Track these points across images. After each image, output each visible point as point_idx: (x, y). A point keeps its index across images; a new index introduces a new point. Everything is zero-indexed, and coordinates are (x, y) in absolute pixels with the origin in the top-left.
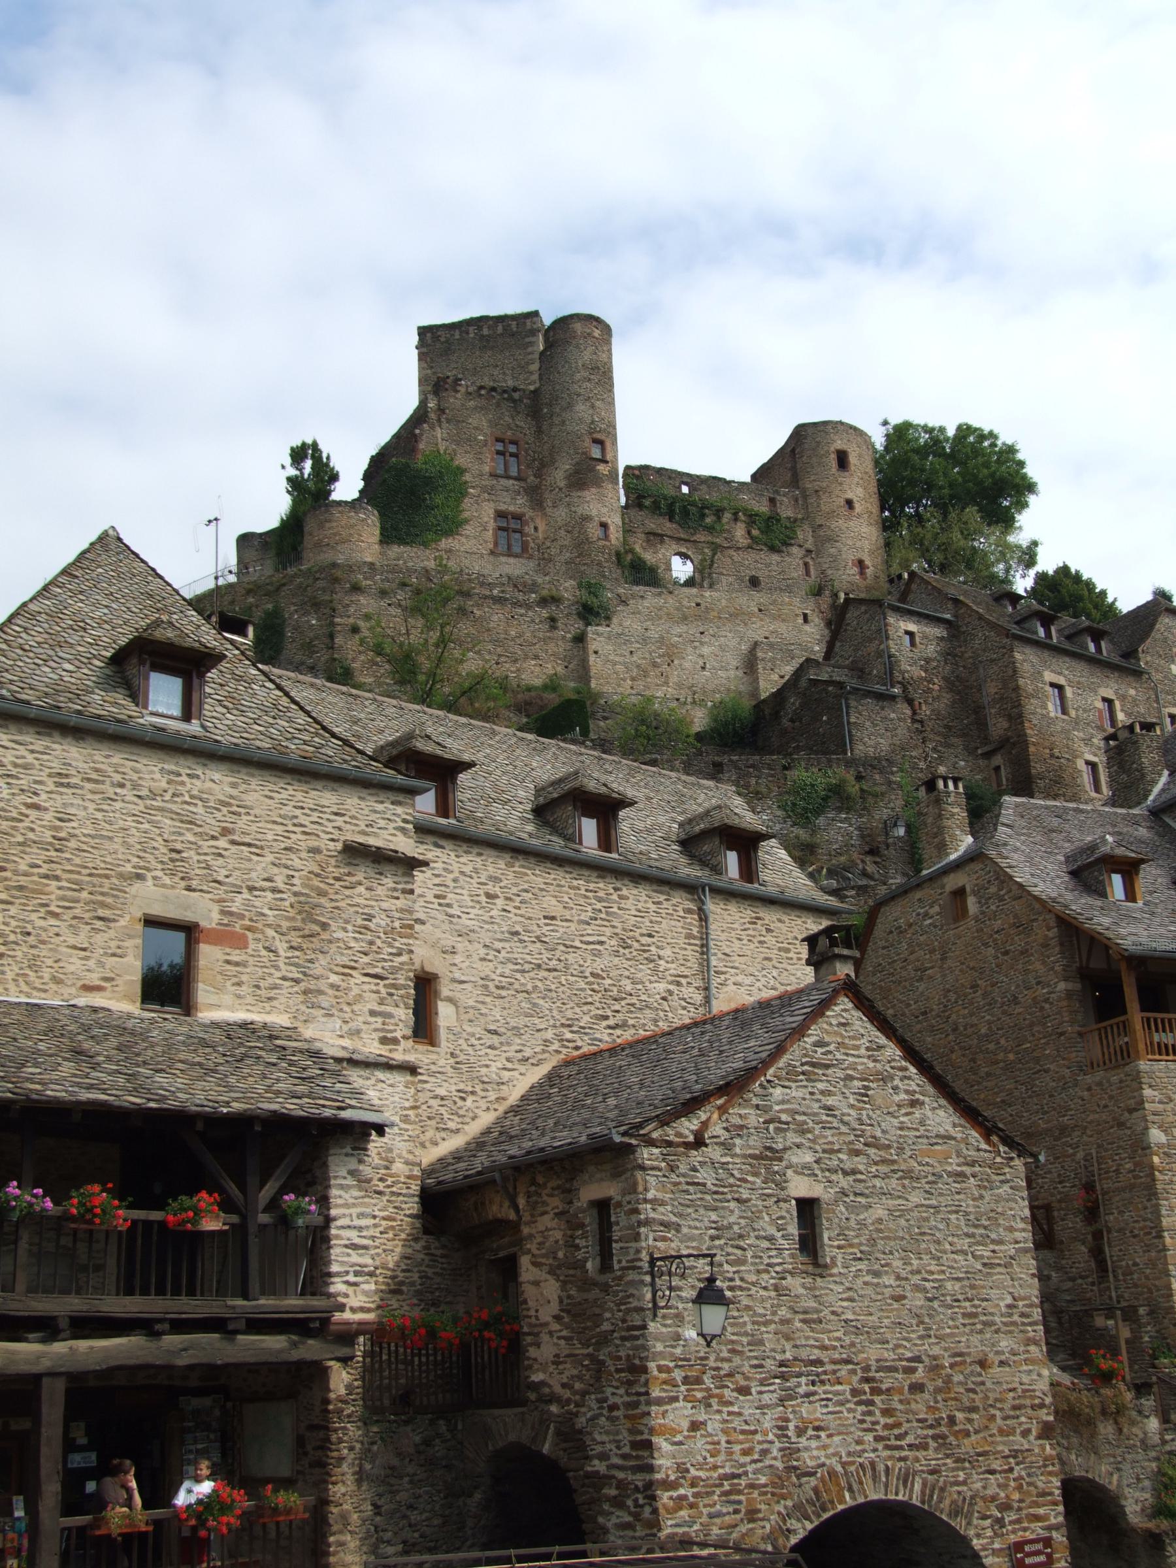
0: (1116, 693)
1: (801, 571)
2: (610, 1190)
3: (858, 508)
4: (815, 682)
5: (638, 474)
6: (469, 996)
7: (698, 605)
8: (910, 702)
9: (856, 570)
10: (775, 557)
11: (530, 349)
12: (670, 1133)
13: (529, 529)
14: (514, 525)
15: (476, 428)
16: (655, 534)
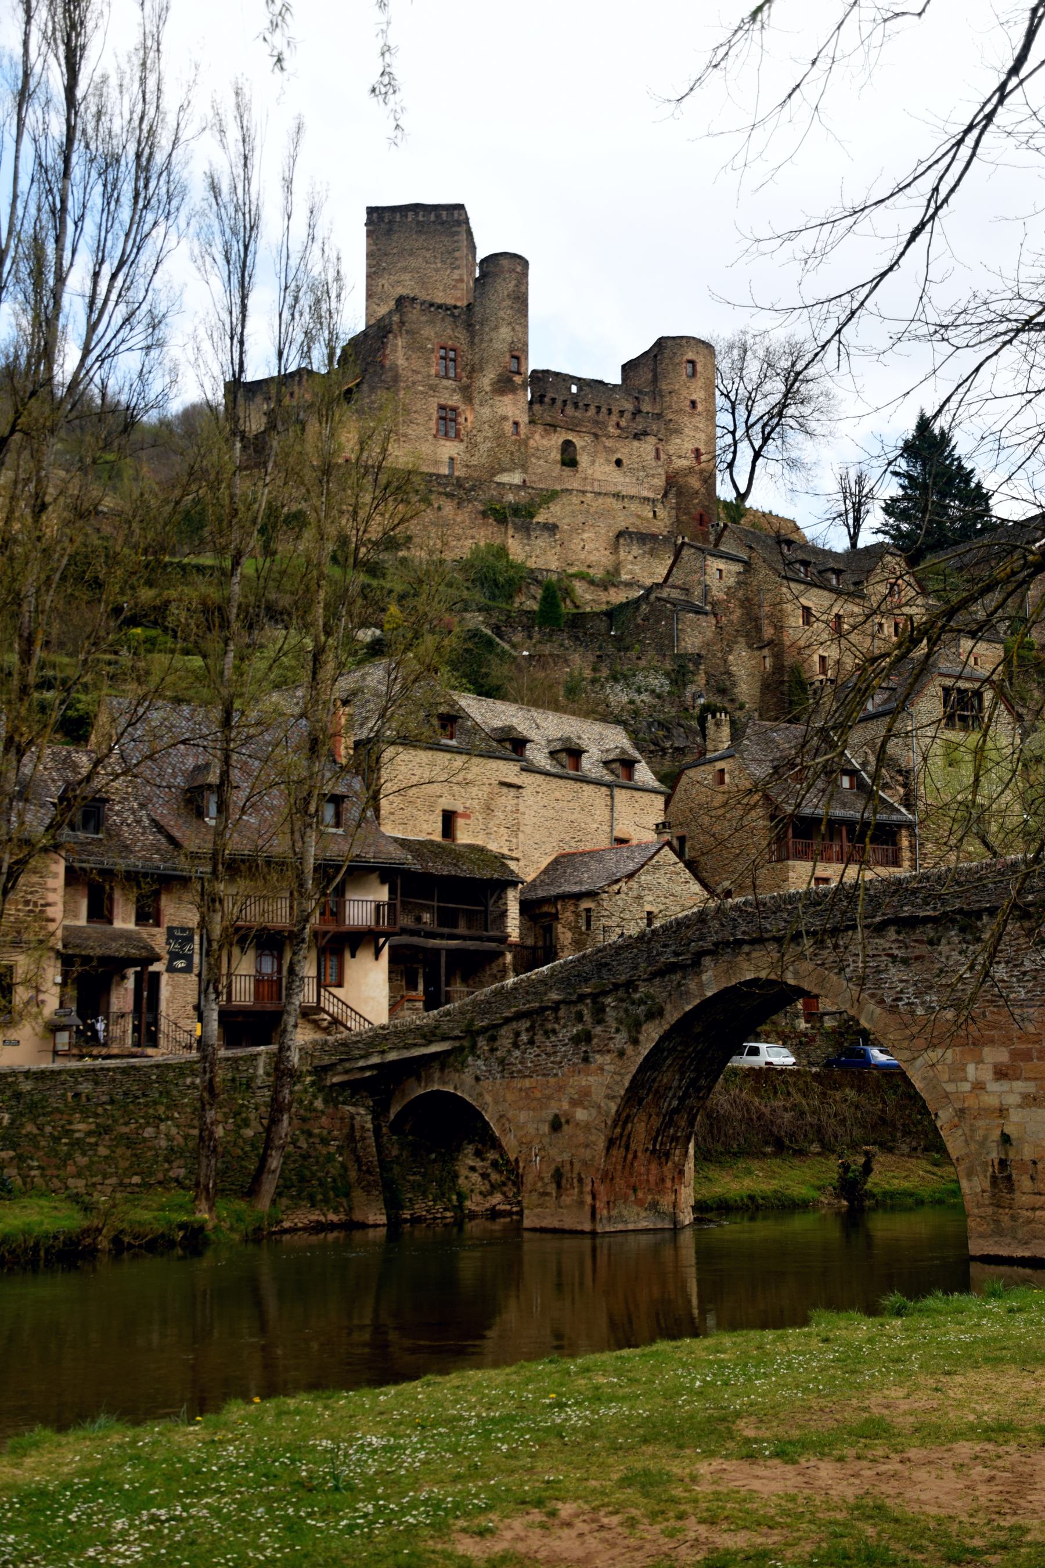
1: (653, 454)
2: (591, 905)
3: (700, 408)
4: (658, 599)
5: (541, 377)
6: (528, 830)
8: (715, 615)
12: (610, 889)
13: (461, 420)
14: (451, 415)
15: (427, 339)
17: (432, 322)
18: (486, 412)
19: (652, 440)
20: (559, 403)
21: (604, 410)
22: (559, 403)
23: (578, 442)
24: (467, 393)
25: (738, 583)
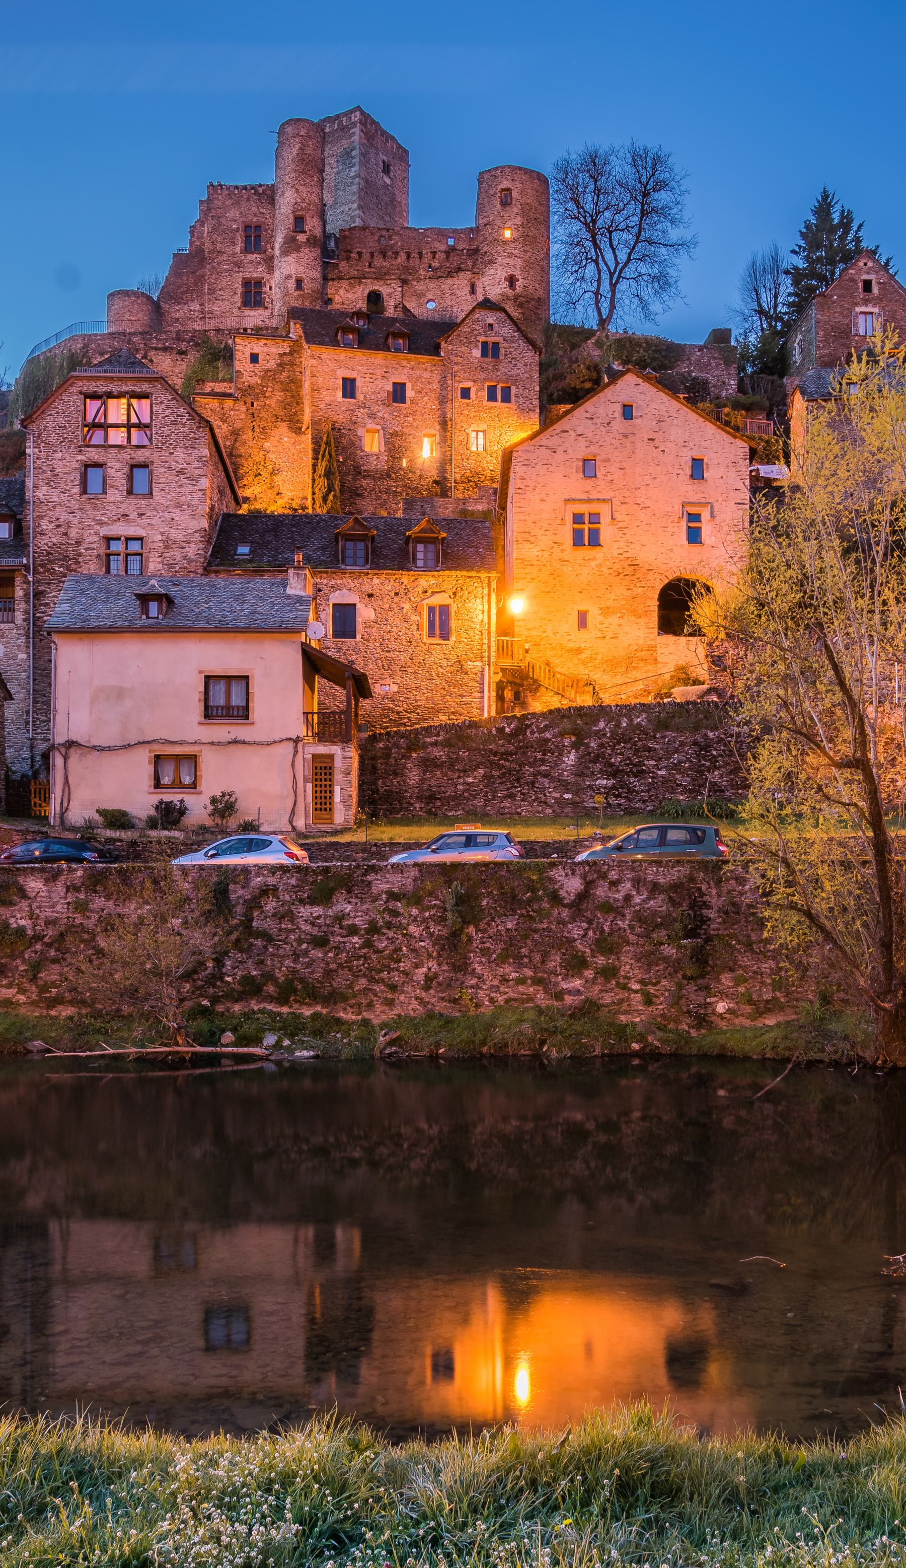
0: (410, 378)
13: (266, 289)
17: (237, 203)
20: (366, 256)
21: (415, 255)
22: (366, 256)
23: (384, 290)
25: (280, 365)
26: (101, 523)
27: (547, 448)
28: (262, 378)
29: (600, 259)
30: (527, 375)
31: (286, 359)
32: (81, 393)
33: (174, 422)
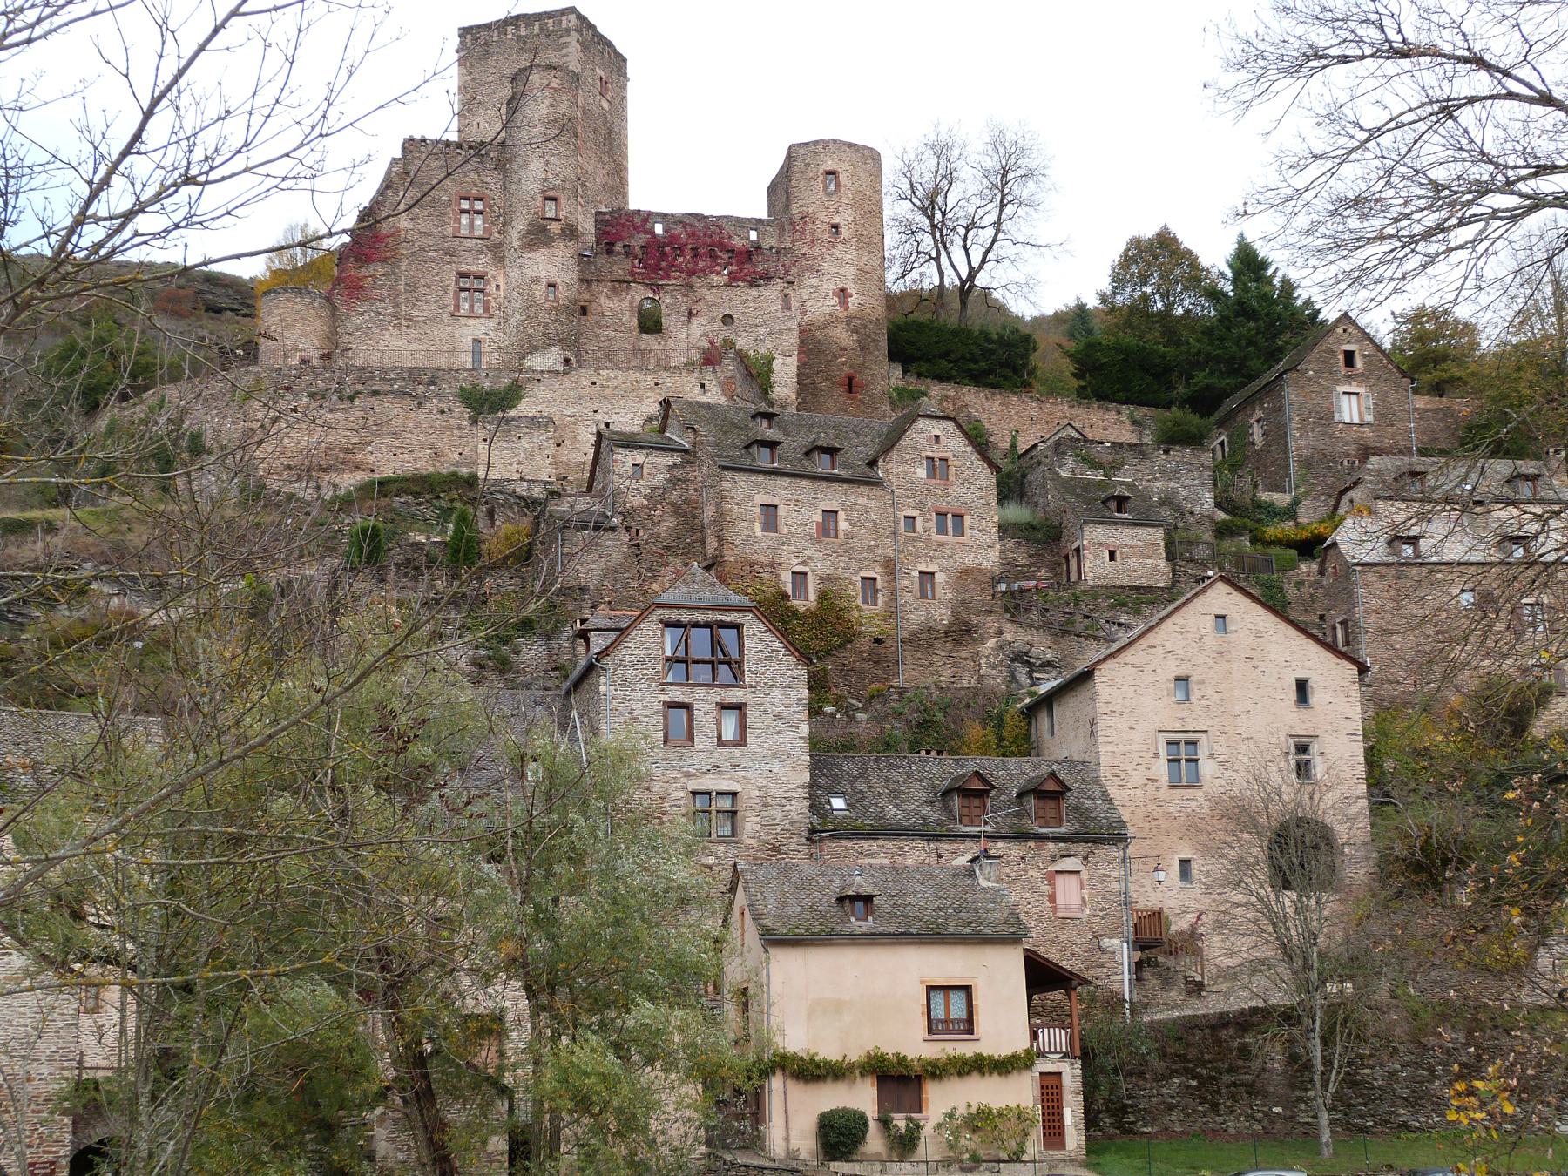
0: (843, 505)
3: (845, 233)
7: (594, 383)
8: (628, 529)
9: (834, 301)
10: (754, 292)
11: (564, 51)
13: (491, 289)
16: (620, 282)
18: (515, 274)
19: (779, 284)
24: (497, 252)
25: (669, 481)
26: (689, 776)
27: (1133, 666)
28: (649, 498)
29: (944, 258)
30: (984, 501)
31: (678, 473)
32: (661, 621)
33: (769, 659)
